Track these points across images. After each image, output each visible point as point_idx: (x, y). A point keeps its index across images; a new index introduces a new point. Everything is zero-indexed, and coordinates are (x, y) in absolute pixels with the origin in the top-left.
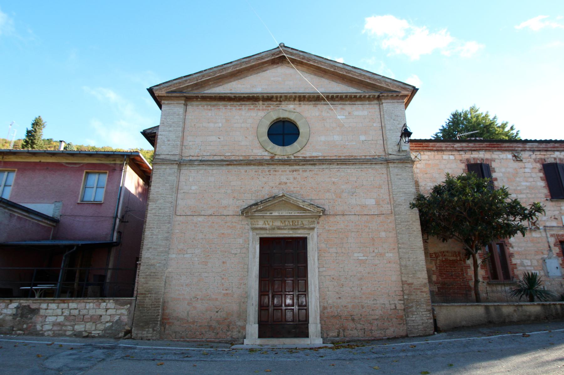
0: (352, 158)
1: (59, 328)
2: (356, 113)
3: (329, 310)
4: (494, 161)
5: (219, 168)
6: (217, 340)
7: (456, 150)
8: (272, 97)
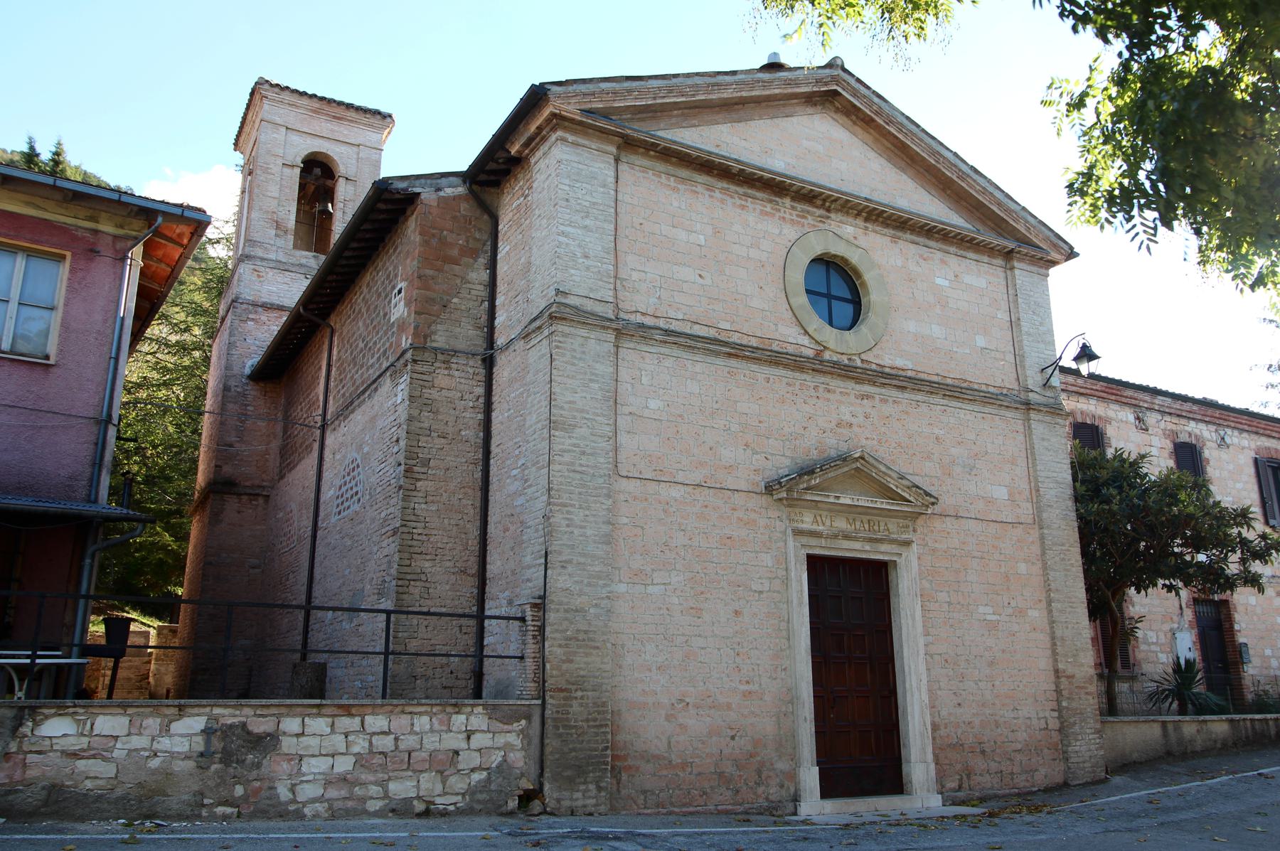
0: (965, 385)
1: (344, 793)
2: (968, 279)
5: (709, 359)
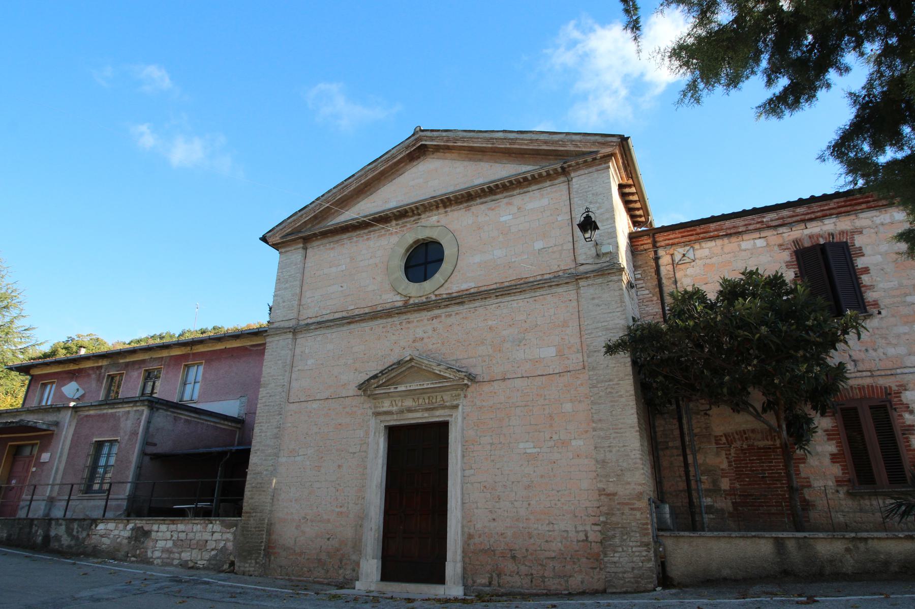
0: (522, 282)
1: (167, 556)
2: (530, 206)
3: (477, 540)
4: (861, 233)
5: (339, 329)
6: (326, 581)
7: (769, 227)
8: (406, 211)
